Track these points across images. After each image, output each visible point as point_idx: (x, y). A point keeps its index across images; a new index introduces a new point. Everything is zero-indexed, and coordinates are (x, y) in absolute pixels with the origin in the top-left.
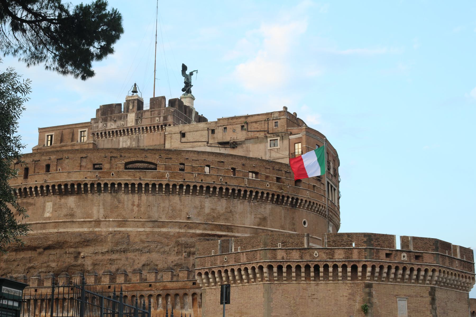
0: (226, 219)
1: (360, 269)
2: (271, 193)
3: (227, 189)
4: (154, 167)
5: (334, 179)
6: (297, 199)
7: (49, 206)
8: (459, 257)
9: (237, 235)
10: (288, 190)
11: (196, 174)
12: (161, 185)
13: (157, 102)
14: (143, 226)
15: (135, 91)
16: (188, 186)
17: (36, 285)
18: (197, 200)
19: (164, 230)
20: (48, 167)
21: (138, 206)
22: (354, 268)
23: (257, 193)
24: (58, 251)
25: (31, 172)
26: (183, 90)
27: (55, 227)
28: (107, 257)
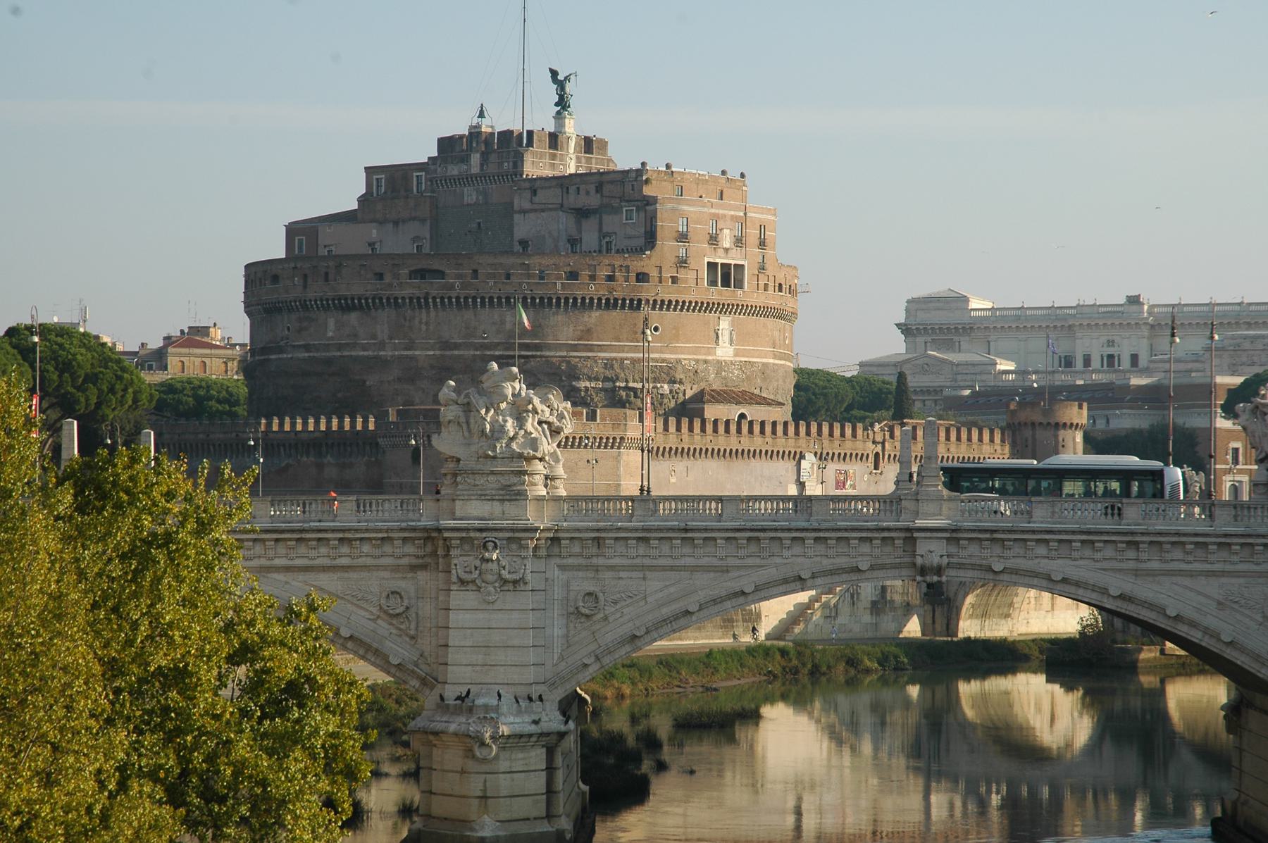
3: (533, 299)
4: (441, 274)
7: (331, 323)
9: (548, 353)
10: (621, 290)
11: (491, 283)
15: (481, 115)
16: (483, 299)
18: (496, 314)
19: (456, 352)
20: (327, 274)
21: (427, 324)
23: (575, 299)
25: (309, 280)
26: (557, 105)
27: (339, 350)
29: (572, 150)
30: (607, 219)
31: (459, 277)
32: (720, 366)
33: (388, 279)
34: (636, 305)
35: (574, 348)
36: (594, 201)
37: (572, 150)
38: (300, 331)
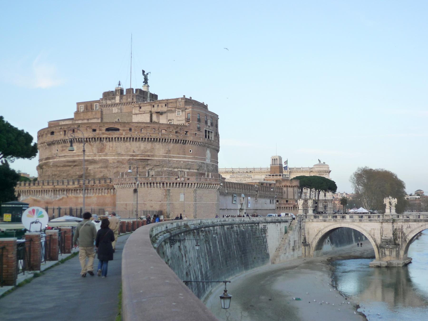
0: (151, 152)
1: (165, 184)
2: (172, 139)
3: (151, 139)
5: (211, 128)
6: (186, 141)
8: (210, 177)
9: (156, 158)
10: (181, 137)
11: (136, 133)
12: (121, 138)
13: (130, 91)
14: (114, 156)
15: (119, 85)
17: (66, 184)
18: (137, 144)
19: (123, 158)
21: (112, 147)
22: (163, 184)
23: (165, 139)
24: (79, 167)
25: (67, 132)
26: (144, 82)
27: (78, 157)
28: (100, 170)
29: (149, 97)
30: (169, 114)
31: (124, 130)
32: (207, 165)
33: (97, 132)
34: (185, 142)
35: (165, 157)
36: (165, 109)
37: (149, 97)
38: (62, 150)
